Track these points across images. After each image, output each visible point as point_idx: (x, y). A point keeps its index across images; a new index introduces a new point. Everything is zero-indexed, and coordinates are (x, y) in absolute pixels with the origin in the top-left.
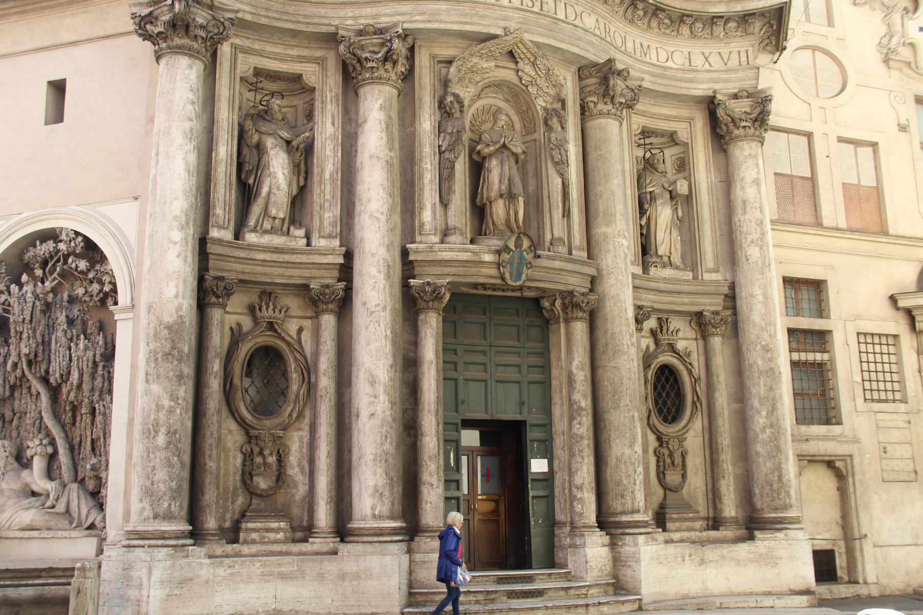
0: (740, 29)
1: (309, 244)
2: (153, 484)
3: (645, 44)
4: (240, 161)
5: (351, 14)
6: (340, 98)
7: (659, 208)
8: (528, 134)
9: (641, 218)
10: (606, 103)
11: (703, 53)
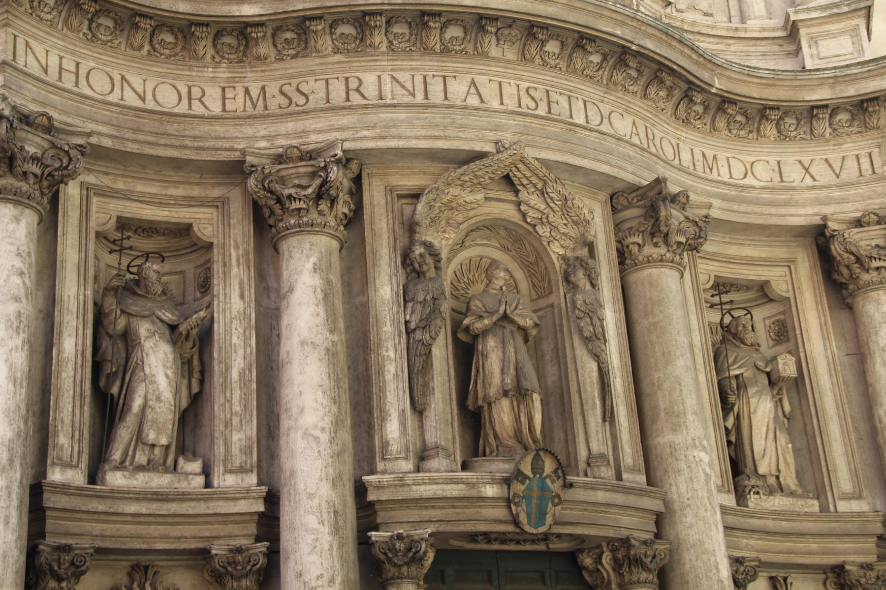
0: (856, 123)
1: (208, 484)
3: (709, 154)
4: (98, 359)
5: (263, 133)
6: (252, 256)
7: (753, 401)
8: (540, 297)
9: (725, 417)
10: (656, 245)
11: (800, 162)
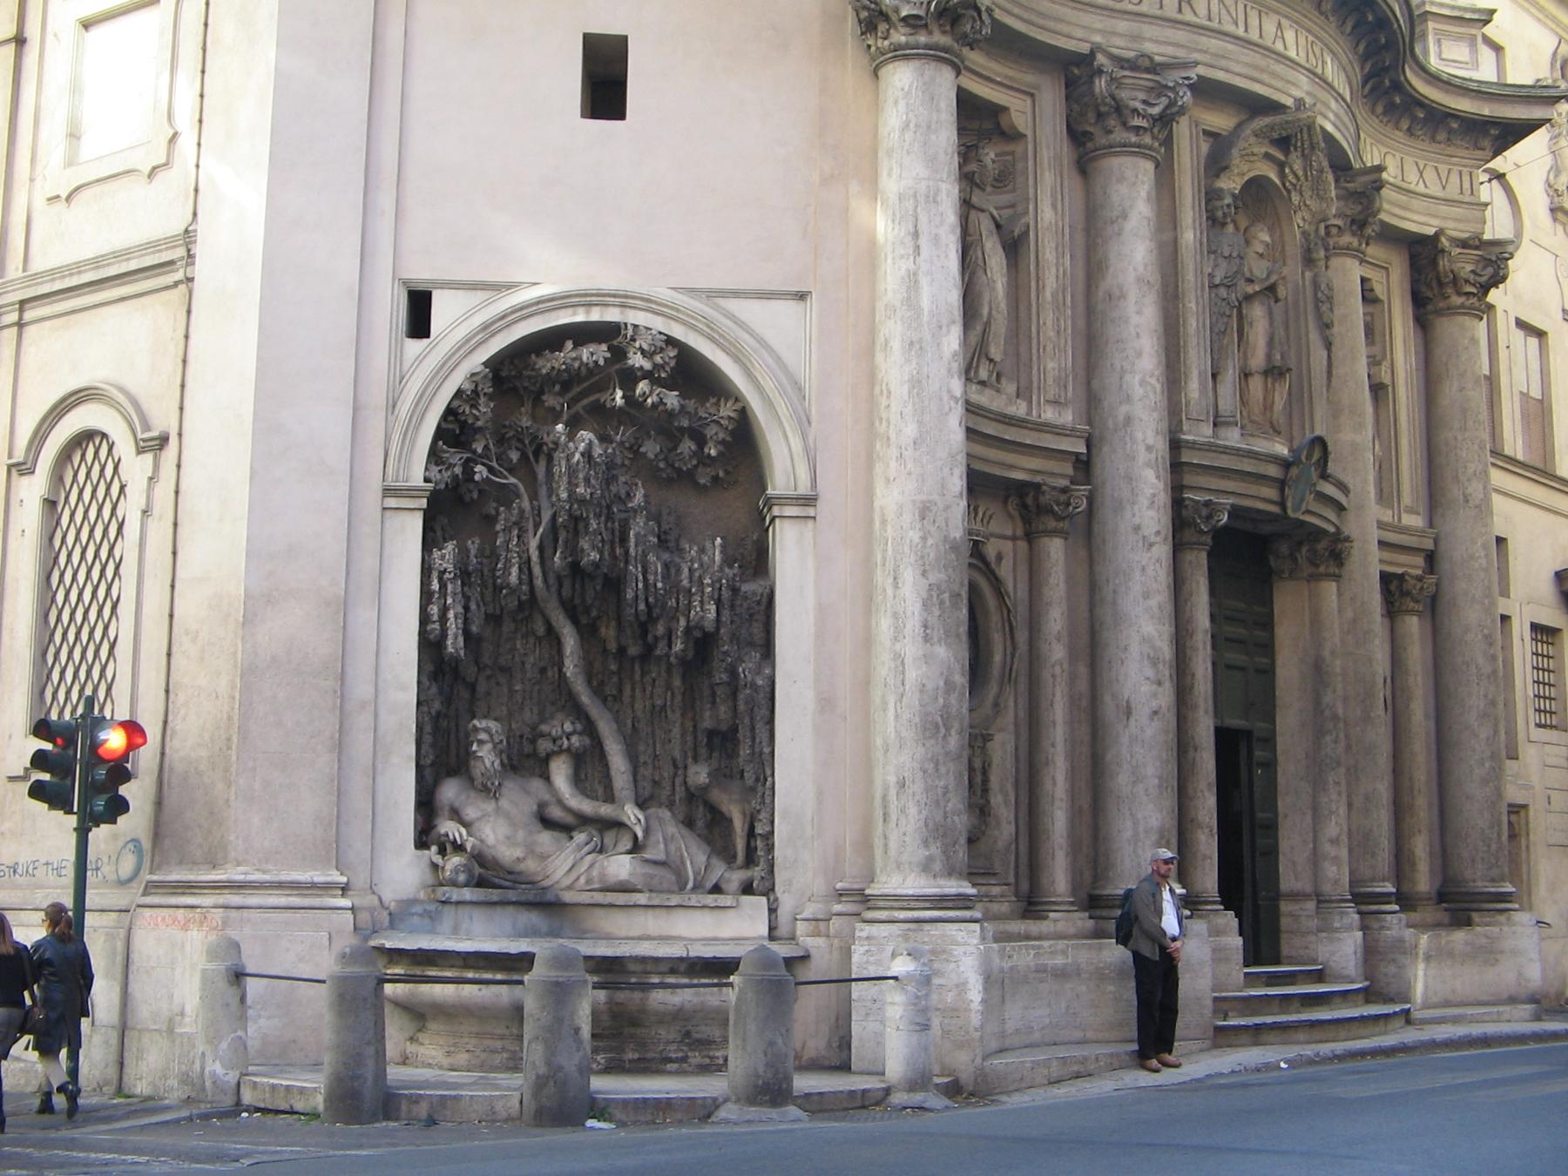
2: (946, 817)
5: (1099, 26)
10: (1354, 234)
